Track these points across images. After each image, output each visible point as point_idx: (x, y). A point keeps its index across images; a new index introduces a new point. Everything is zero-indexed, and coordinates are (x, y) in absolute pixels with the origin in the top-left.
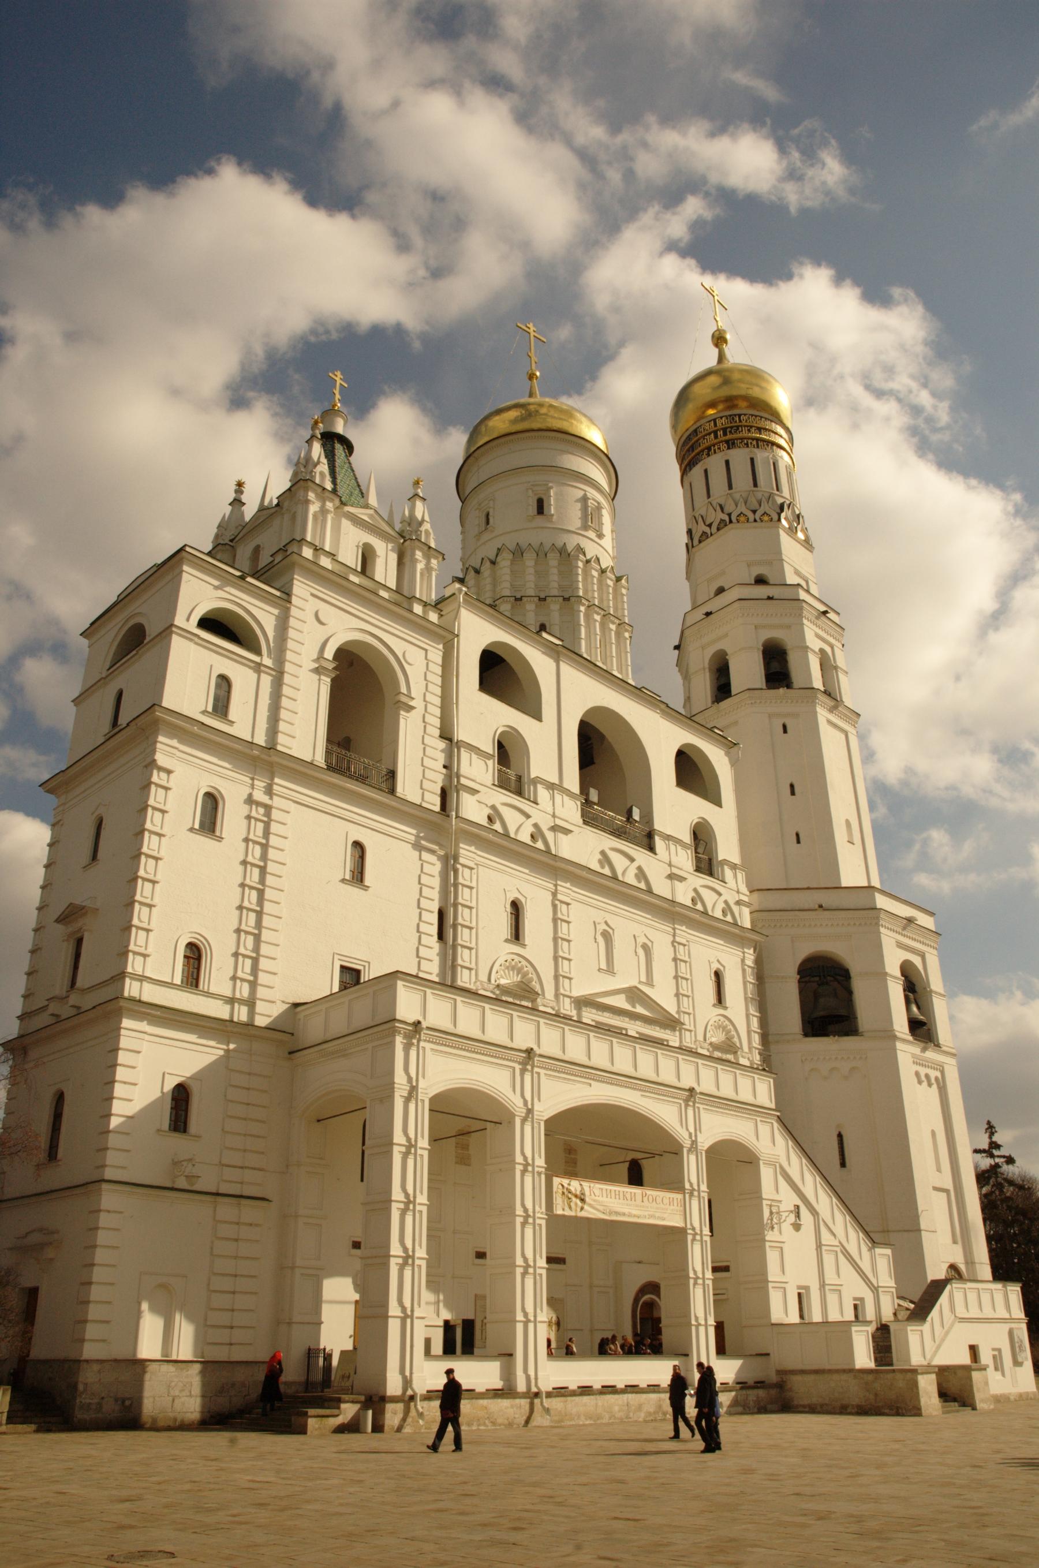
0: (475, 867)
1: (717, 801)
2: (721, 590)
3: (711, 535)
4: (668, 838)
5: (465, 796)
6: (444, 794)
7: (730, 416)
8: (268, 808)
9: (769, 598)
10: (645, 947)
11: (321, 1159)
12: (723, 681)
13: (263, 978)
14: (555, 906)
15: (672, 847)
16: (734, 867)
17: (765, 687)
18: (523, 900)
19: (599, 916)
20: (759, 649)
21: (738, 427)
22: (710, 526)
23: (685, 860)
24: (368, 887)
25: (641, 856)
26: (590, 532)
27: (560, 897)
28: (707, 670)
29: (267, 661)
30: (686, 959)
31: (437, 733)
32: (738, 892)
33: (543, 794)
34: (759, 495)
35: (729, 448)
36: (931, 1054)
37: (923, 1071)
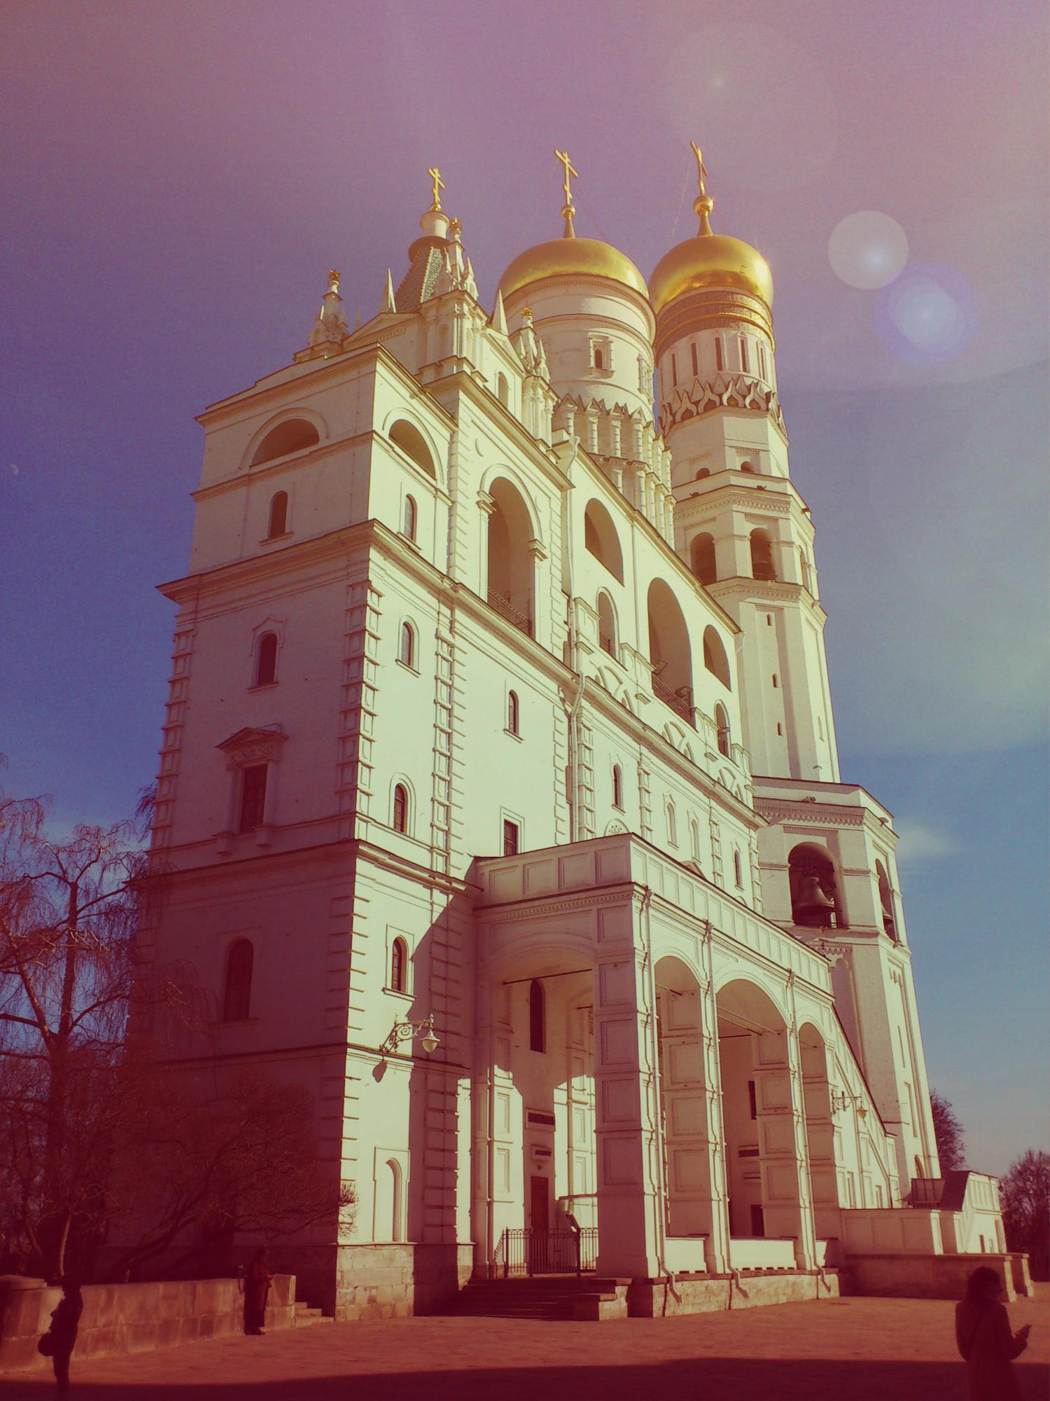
2: (704, 474)
3: (698, 414)
5: (583, 654)
8: (451, 646)
9: (760, 488)
11: (508, 1024)
13: (455, 828)
17: (752, 577)
18: (621, 766)
20: (745, 537)
26: (643, 395)
28: (689, 552)
29: (439, 486)
33: (628, 660)
36: (896, 952)
37: (894, 968)
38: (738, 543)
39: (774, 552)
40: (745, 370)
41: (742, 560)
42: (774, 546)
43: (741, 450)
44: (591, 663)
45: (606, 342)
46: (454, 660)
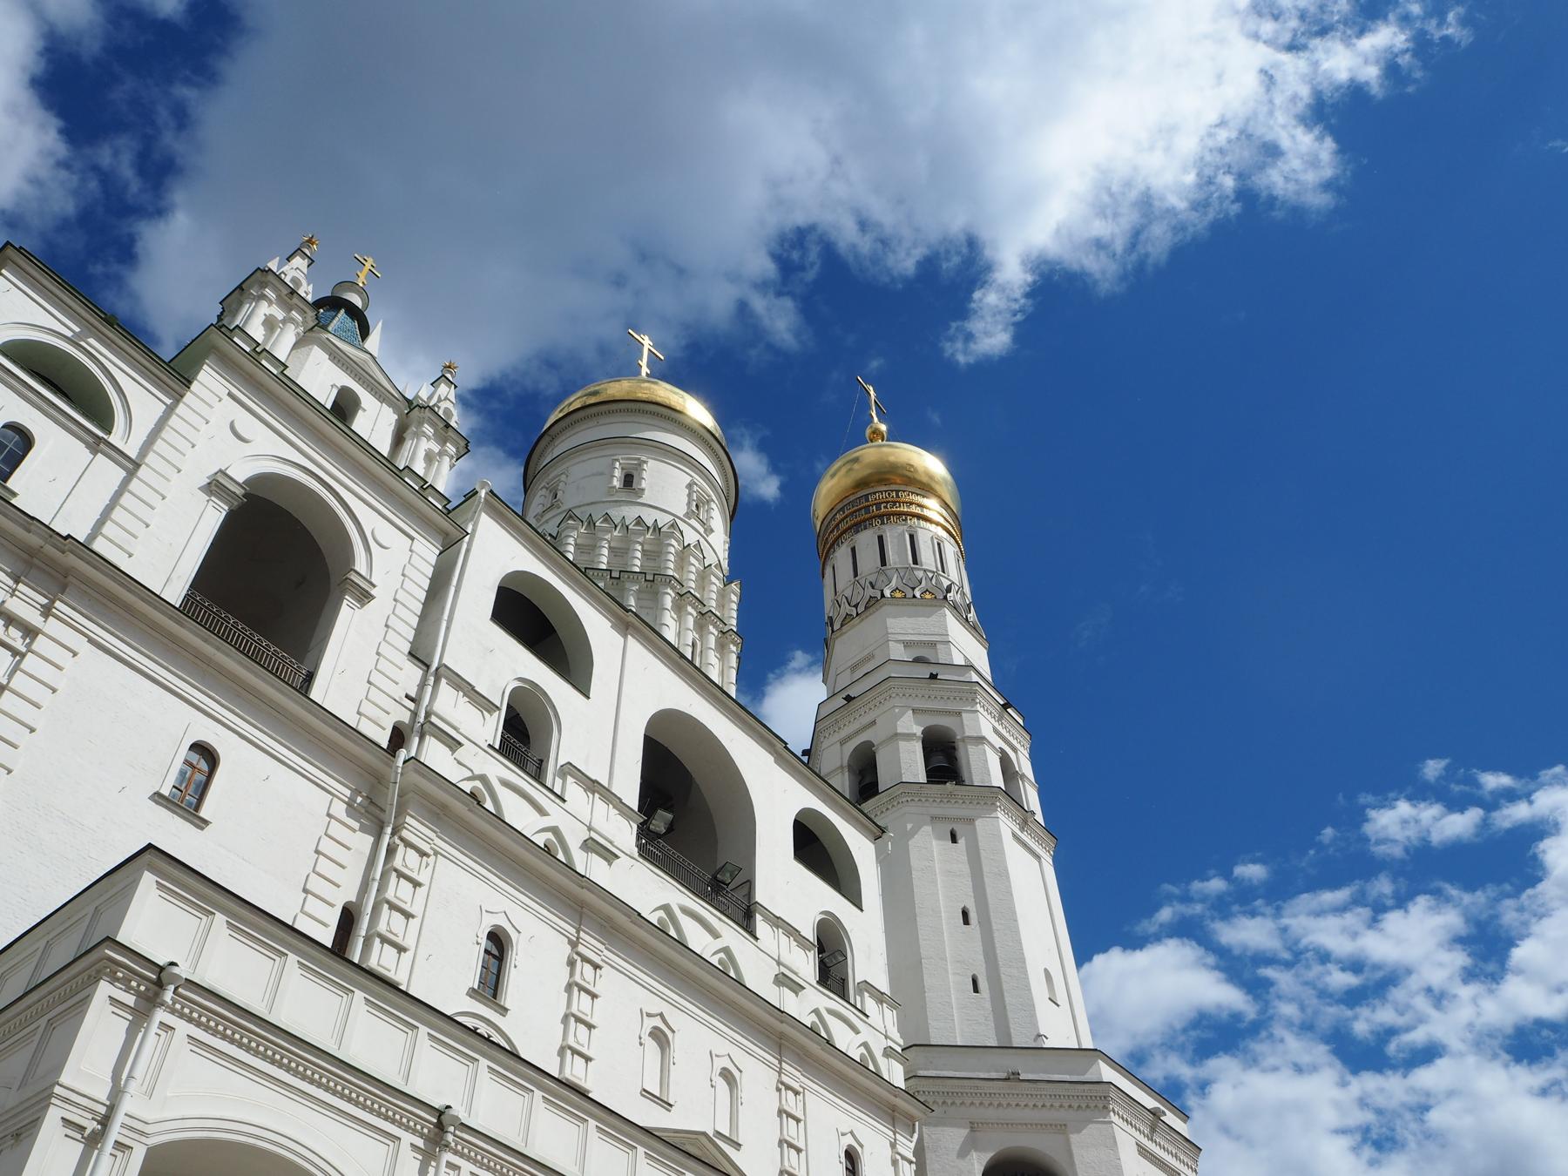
0: (431, 852)
1: (853, 896)
3: (857, 614)
4: (777, 922)
6: (399, 737)
7: (886, 491)
10: (726, 1074)
12: (868, 780)
14: (571, 963)
15: (784, 939)
16: (880, 997)
19: (656, 1005)
21: (895, 503)
22: (856, 606)
23: (805, 965)
24: (206, 822)
25: (731, 935)
27: (581, 949)
30: (799, 1114)
31: (406, 647)
32: (886, 1037)
33: (574, 791)
34: (920, 574)
35: (883, 523)
38: (902, 744)
39: (961, 753)
40: (915, 561)
41: (911, 763)
42: (960, 746)
43: (908, 645)
44: (459, 763)
45: (641, 463)
46: (30, 650)
